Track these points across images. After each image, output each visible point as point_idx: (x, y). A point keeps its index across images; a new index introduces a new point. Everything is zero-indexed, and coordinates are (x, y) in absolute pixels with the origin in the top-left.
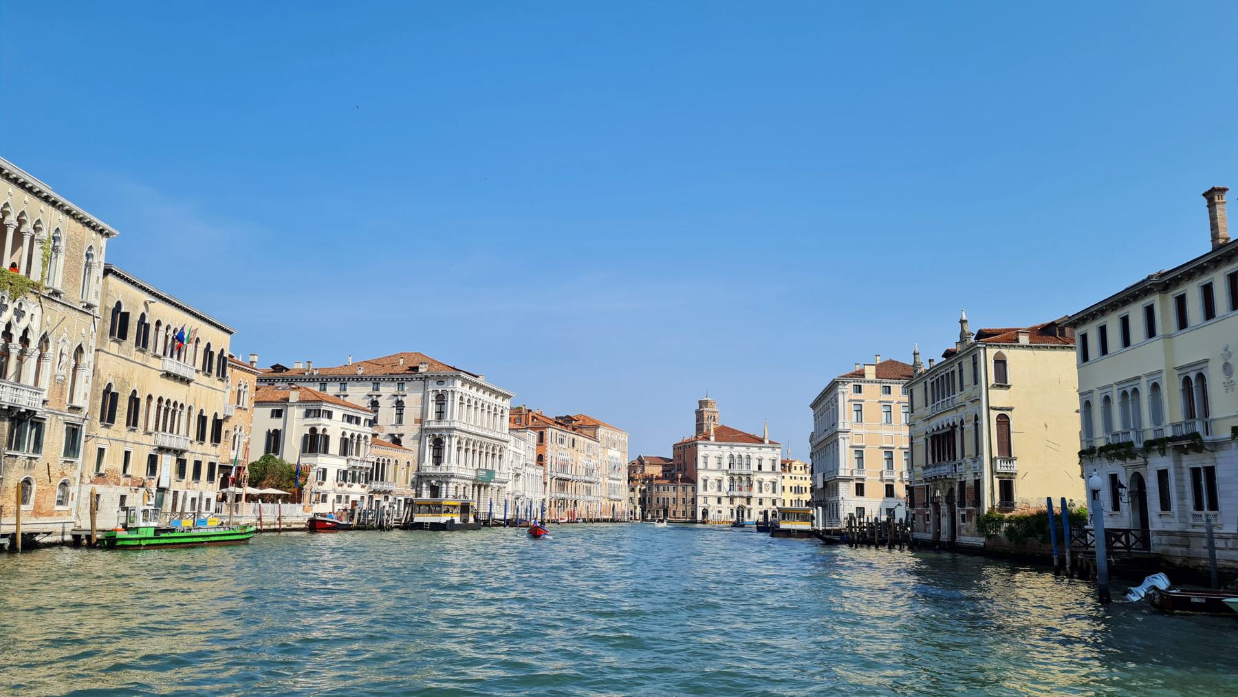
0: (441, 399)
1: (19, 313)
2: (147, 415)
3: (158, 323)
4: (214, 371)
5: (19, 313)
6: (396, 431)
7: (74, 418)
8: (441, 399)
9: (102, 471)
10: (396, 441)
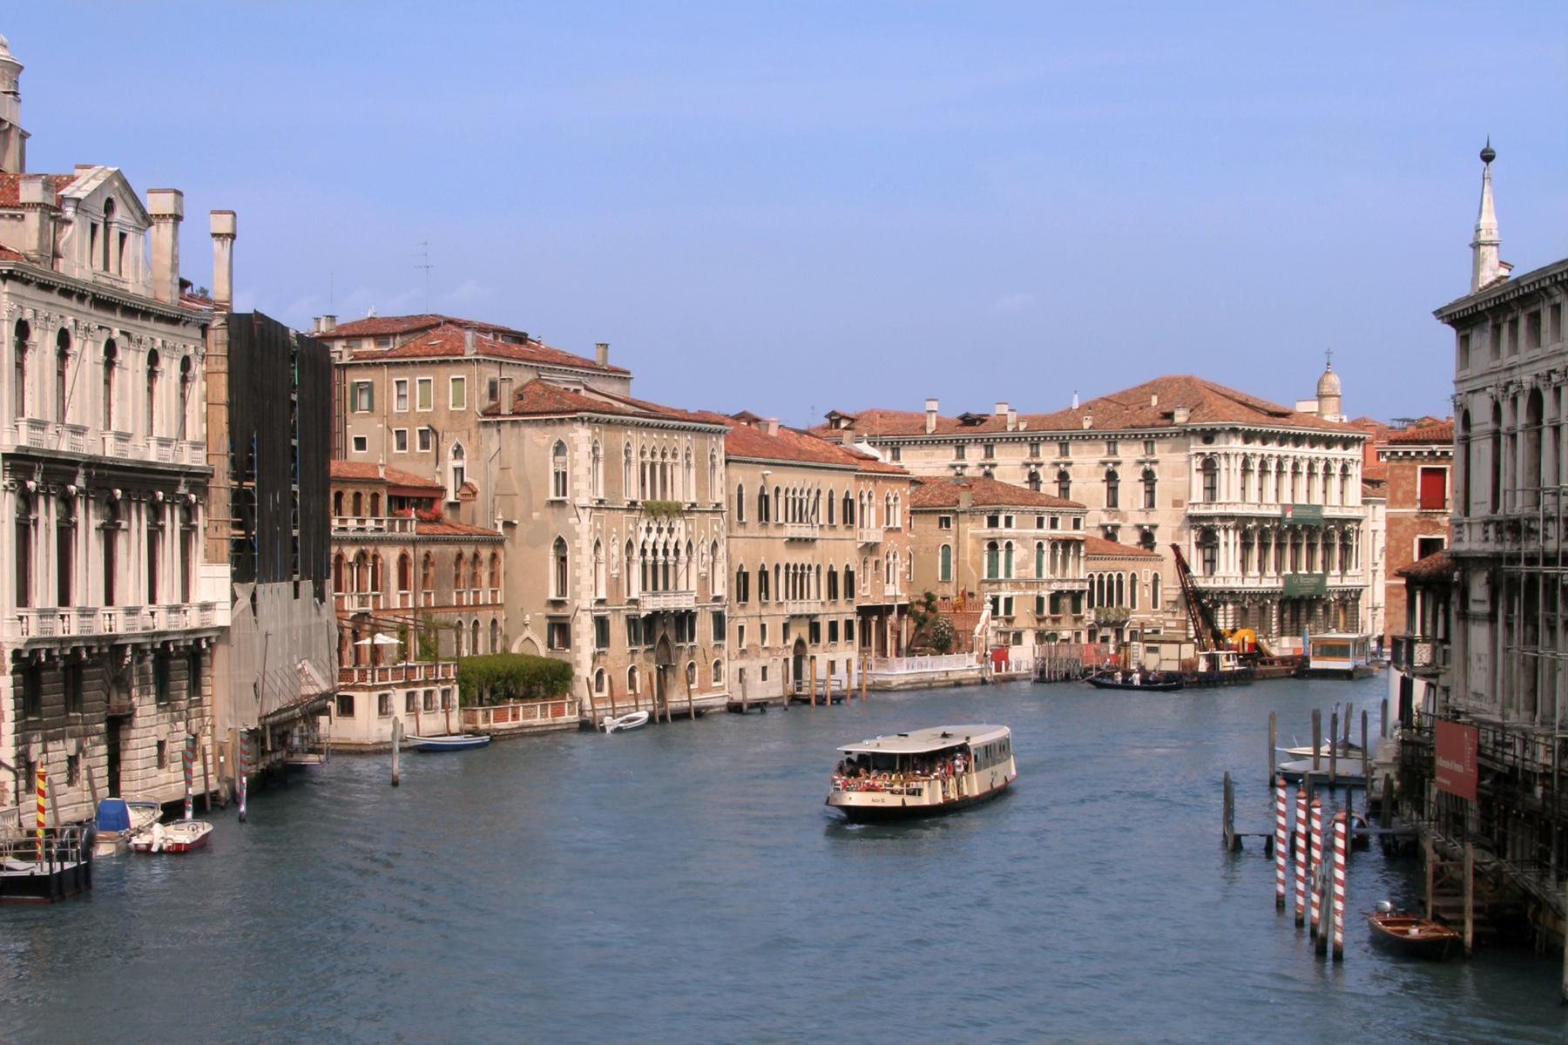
0: (1209, 467)
2: (779, 585)
3: (777, 490)
5: (671, 531)
6: (1144, 521)
8: (1209, 467)
9: (744, 647)
10: (1147, 538)
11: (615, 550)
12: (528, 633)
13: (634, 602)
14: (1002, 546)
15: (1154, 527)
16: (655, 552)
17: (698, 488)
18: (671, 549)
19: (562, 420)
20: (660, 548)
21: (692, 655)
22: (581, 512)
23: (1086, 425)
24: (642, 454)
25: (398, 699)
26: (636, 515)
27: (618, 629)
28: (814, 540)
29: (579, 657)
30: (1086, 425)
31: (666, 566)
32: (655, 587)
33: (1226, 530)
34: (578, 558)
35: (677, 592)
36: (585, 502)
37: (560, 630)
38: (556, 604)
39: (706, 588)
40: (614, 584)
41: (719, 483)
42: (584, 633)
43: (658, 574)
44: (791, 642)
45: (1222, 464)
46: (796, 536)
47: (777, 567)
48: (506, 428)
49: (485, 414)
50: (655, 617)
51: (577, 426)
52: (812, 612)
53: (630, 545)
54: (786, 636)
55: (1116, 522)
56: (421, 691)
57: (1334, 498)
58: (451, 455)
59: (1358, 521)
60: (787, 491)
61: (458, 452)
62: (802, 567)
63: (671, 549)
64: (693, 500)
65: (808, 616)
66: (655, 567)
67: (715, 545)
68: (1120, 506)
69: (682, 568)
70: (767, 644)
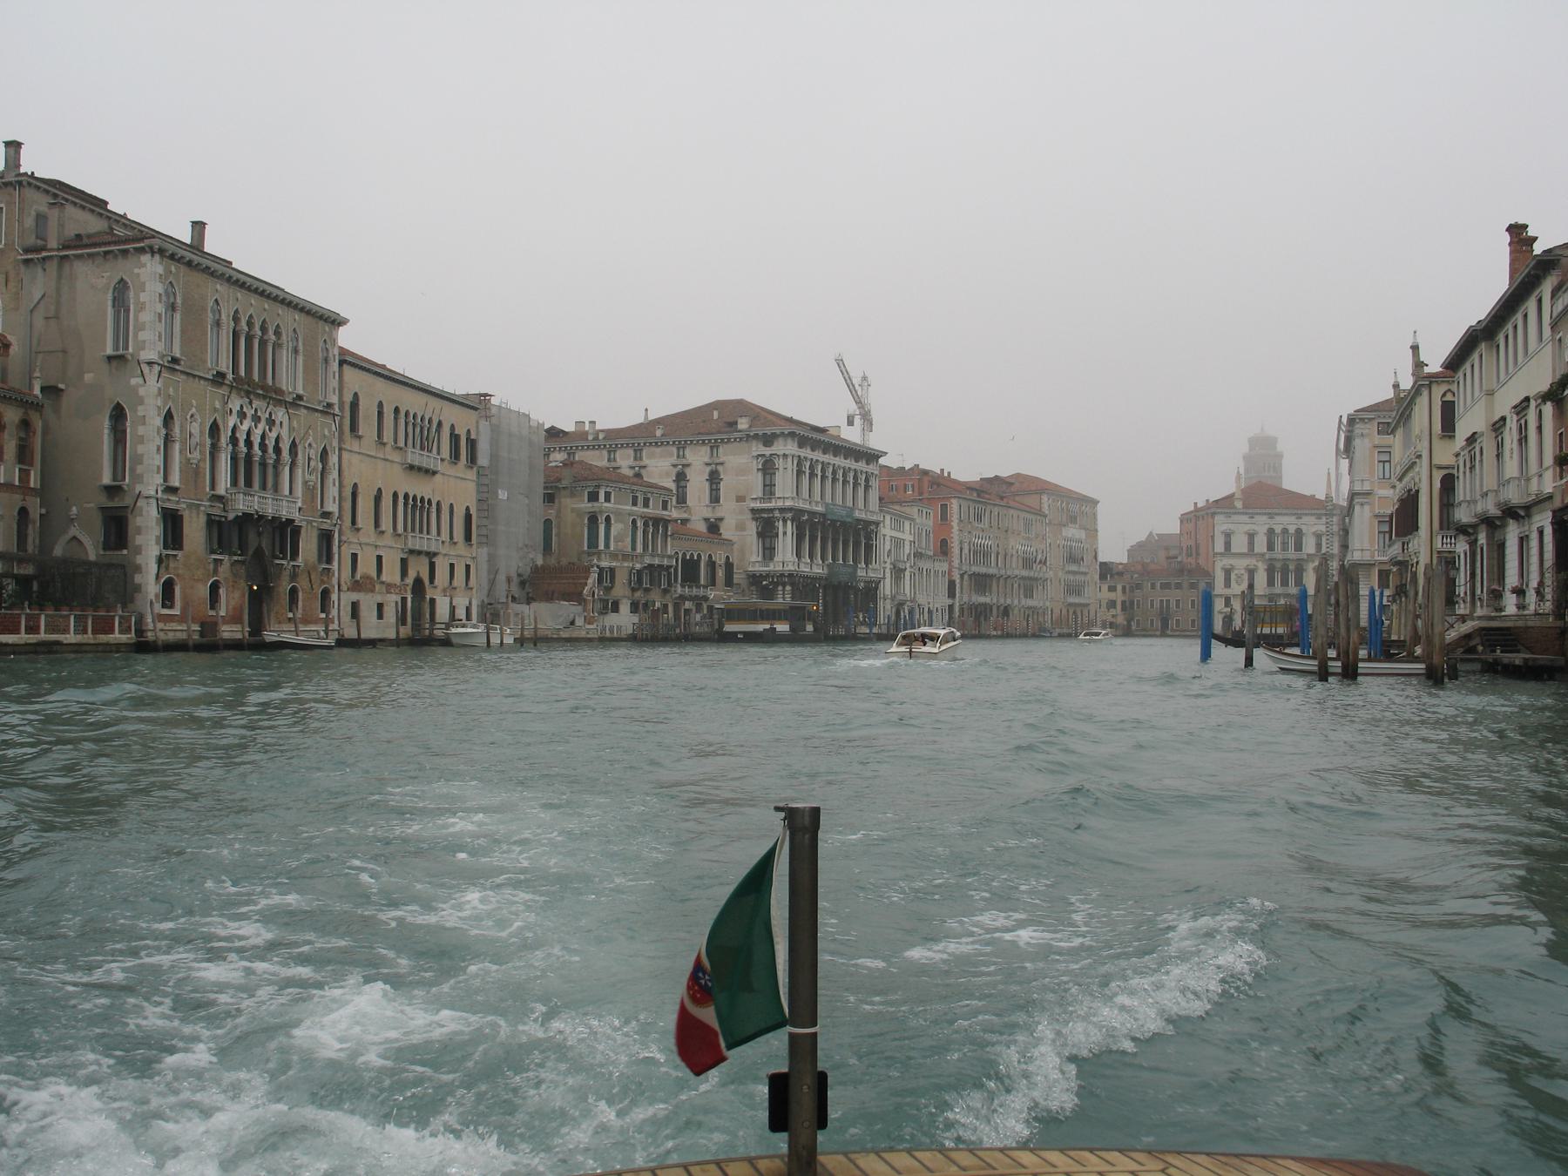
0: (768, 468)
1: (271, 422)
7: (326, 525)
8: (768, 468)
9: (358, 577)
11: (195, 428)
12: (74, 531)
13: (220, 498)
14: (602, 519)
15: (721, 519)
16: (249, 443)
18: (271, 444)
19: (125, 252)
22: (146, 369)
23: (659, 433)
26: (224, 391)
27: (195, 531)
28: (434, 473)
29: (139, 560)
30: (659, 433)
31: (263, 465)
32: (249, 483)
33: (785, 521)
34: (141, 430)
36: (153, 356)
37: (117, 528)
38: (113, 491)
40: (191, 472)
44: (410, 580)
45: (779, 463)
46: (416, 463)
48: (52, 267)
49: (27, 251)
50: (246, 519)
51: (146, 258)
52: (433, 549)
53: (215, 429)
54: (404, 573)
55: (685, 516)
57: (861, 503)
59: (877, 524)
62: (422, 499)
63: (271, 444)
67: (324, 454)
70: (384, 578)
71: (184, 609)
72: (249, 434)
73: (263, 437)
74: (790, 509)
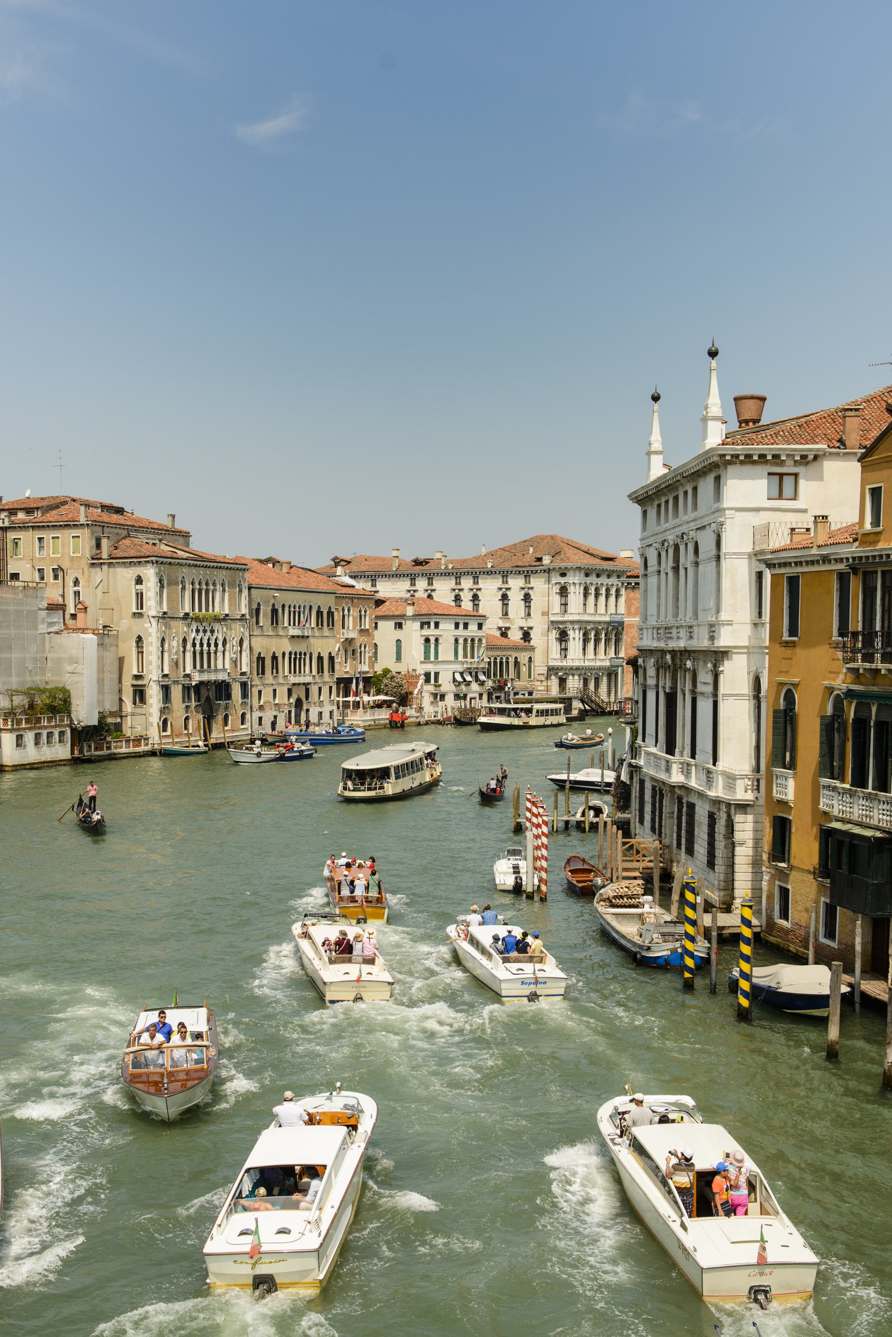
0: (563, 591)
3: (283, 606)
4: (325, 624)
5: (212, 631)
6: (525, 624)
7: (244, 679)
8: (563, 591)
10: (526, 636)
11: (175, 644)
15: (531, 628)
17: (230, 605)
18: (212, 643)
20: (205, 642)
21: (226, 708)
22: (152, 620)
23: (489, 565)
24: (193, 584)
25: (29, 737)
27: (177, 693)
28: (308, 637)
31: (209, 653)
34: (150, 649)
35: (216, 670)
38: (137, 677)
39: (236, 666)
41: (244, 601)
42: (154, 695)
43: (203, 657)
45: (571, 589)
47: (284, 654)
48: (105, 567)
53: (185, 640)
55: (507, 625)
56: (44, 733)
58: (72, 584)
60: (290, 607)
61: (76, 582)
63: (212, 643)
64: (227, 612)
65: (304, 684)
66: (202, 653)
68: (510, 616)
69: (220, 655)
71: (172, 731)
72: (201, 640)
73: (209, 640)
74: (578, 622)
